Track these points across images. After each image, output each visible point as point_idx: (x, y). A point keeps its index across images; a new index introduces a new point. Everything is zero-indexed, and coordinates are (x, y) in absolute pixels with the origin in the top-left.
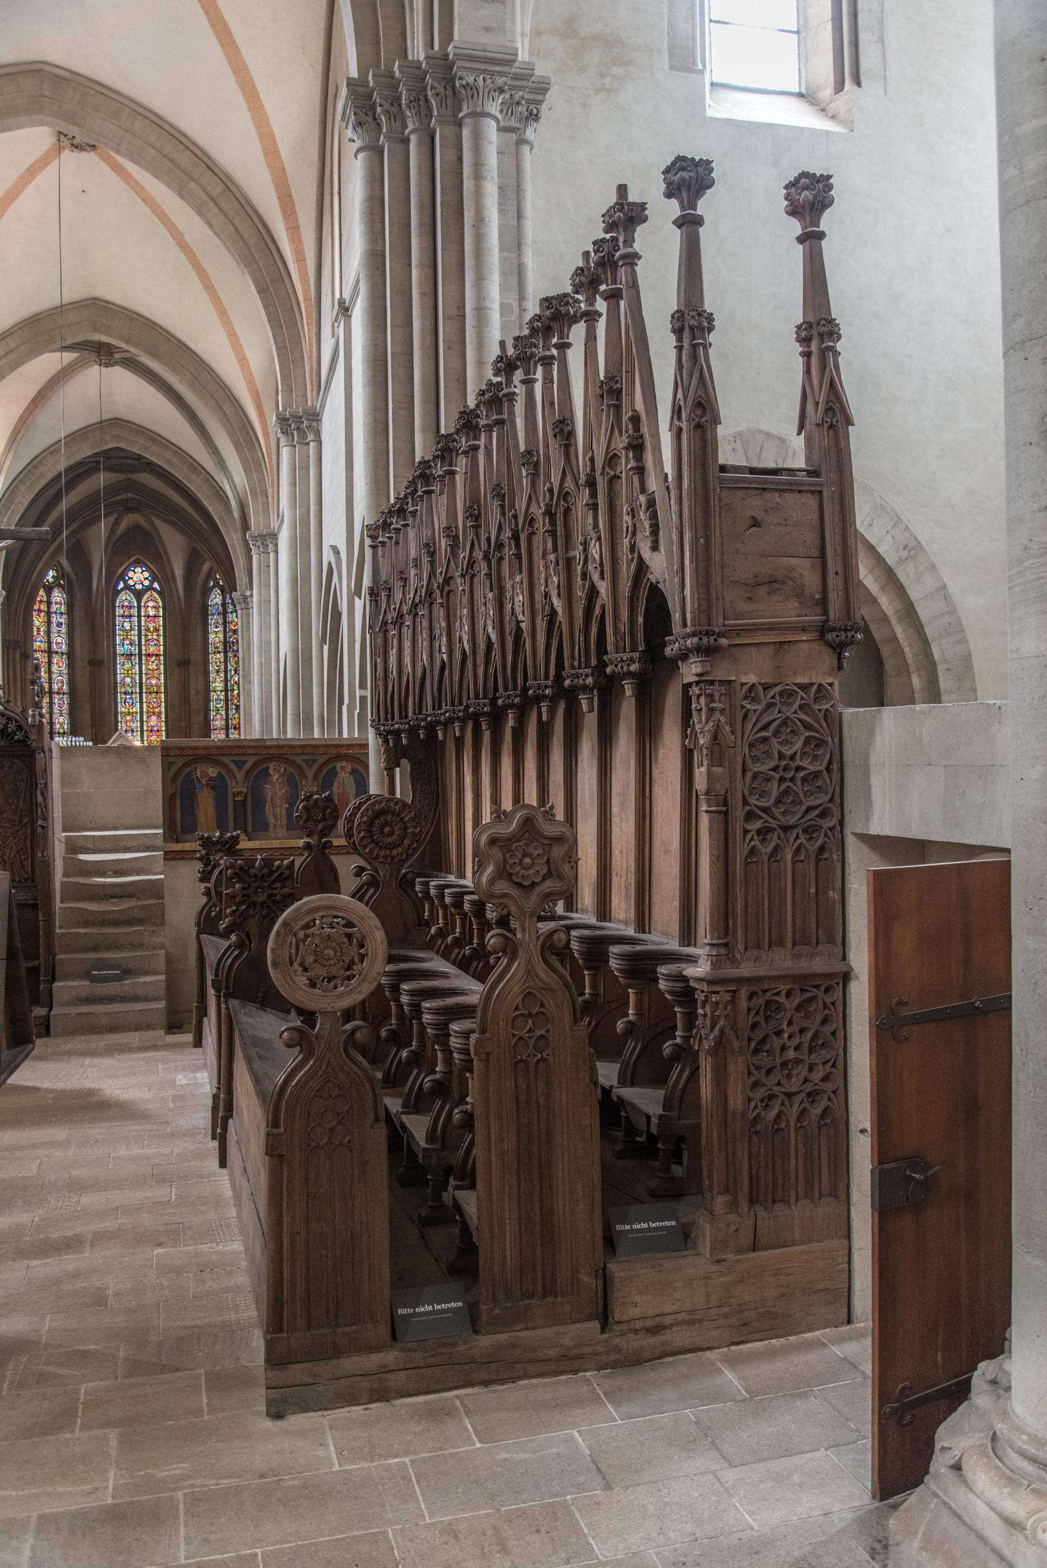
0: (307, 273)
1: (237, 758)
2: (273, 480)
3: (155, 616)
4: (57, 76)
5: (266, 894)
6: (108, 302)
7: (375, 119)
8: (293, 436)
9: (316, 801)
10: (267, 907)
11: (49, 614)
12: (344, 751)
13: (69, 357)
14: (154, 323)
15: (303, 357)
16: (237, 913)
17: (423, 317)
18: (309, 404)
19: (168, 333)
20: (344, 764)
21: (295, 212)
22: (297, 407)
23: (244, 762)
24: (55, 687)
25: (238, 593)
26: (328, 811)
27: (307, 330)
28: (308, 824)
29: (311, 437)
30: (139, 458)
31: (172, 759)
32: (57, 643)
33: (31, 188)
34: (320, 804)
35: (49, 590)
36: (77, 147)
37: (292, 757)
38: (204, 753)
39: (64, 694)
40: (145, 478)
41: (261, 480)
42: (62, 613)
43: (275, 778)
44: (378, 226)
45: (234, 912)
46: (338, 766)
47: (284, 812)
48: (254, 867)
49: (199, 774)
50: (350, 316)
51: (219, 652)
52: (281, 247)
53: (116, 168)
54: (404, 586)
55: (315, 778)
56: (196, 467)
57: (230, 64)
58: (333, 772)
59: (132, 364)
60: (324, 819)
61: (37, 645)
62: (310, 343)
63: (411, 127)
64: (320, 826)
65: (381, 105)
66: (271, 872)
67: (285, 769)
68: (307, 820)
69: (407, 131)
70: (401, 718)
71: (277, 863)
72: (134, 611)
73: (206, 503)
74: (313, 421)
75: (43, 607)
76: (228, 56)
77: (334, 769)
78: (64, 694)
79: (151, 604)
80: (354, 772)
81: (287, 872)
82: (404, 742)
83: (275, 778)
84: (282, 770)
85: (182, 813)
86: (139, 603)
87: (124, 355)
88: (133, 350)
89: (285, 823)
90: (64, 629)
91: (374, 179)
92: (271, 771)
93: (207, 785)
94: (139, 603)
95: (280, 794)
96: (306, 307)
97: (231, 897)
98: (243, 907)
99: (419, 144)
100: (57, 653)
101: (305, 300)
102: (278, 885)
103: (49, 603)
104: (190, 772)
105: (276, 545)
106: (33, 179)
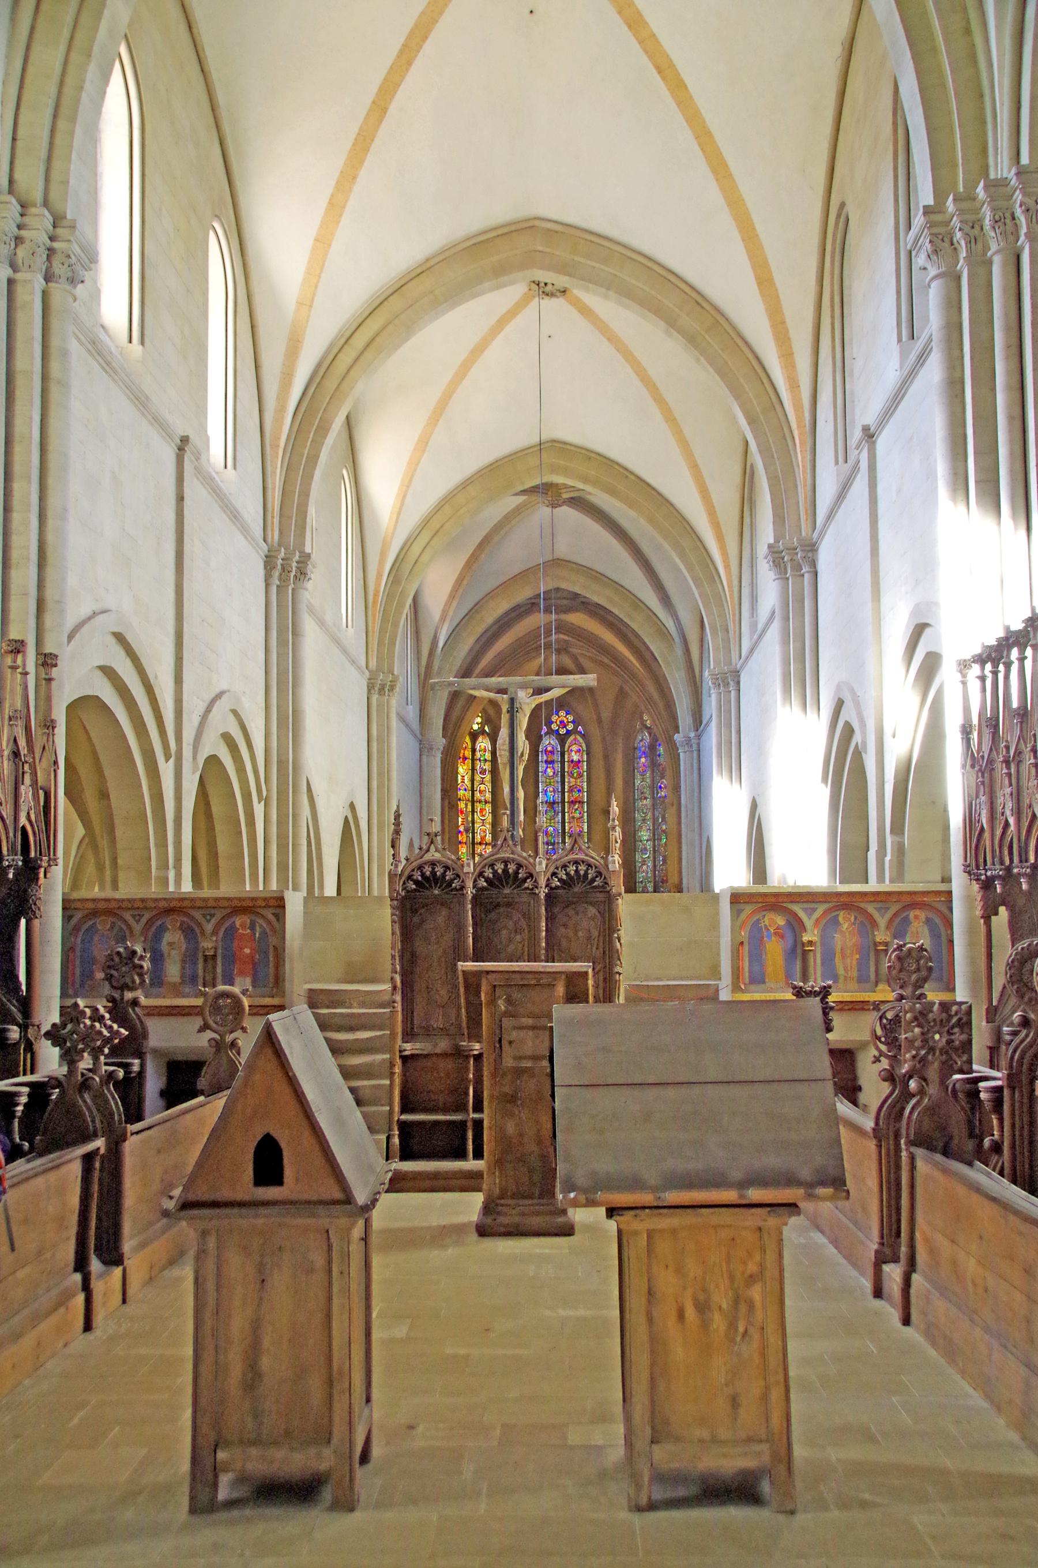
0: (801, 399)
1: (806, 905)
2: (734, 615)
3: (579, 761)
4: (549, 230)
5: (944, 1040)
6: (565, 443)
7: (952, 244)
8: (785, 569)
9: (910, 950)
10: (947, 1053)
11: (473, 760)
12: (918, 899)
13: (521, 499)
14: (612, 461)
15: (796, 486)
16: (918, 1058)
17: (1011, 442)
18: (804, 534)
19: (626, 469)
20: (917, 912)
21: (789, 339)
22: (791, 539)
23: (814, 910)
24: (478, 839)
25: (681, 735)
26: (922, 962)
27: (801, 457)
28: (902, 975)
29: (805, 569)
30: (576, 596)
31: (742, 906)
32: (481, 792)
33: (500, 338)
34: (914, 954)
35: (474, 736)
36: (547, 295)
37: (862, 905)
38: (773, 900)
39: (486, 844)
40: (578, 619)
41: (723, 615)
42: (486, 760)
43: (845, 926)
44: (956, 353)
45: (914, 1057)
46: (912, 914)
47: (855, 963)
48: (932, 1012)
49: (767, 923)
50: (874, 442)
51: (646, 798)
52: (772, 377)
53: (585, 311)
54: (1021, 723)
55: (888, 928)
56: (638, 604)
57: (725, 197)
58: (906, 921)
59: (579, 503)
60: (918, 970)
61: (461, 793)
62: (804, 472)
63: (994, 247)
64: (914, 977)
65: (960, 230)
66: (951, 1017)
67: (856, 918)
68: (900, 971)
69: (989, 254)
70: (1021, 861)
71: (954, 1008)
72: (557, 757)
73: (646, 640)
74: (808, 551)
75: (468, 753)
76: (723, 190)
77: (907, 918)
78: (486, 844)
79: (575, 748)
80: (928, 921)
81: (965, 1019)
82: (1024, 887)
83: (845, 926)
84: (853, 918)
85: (750, 962)
86: (563, 746)
87: (572, 495)
88: (588, 488)
89: (855, 974)
90: (488, 777)
91: (952, 304)
92: (841, 919)
93: (775, 933)
94: (563, 746)
95: (849, 944)
96: (800, 435)
97: (910, 1042)
98: (923, 1052)
99: (1004, 265)
100: (480, 802)
101: (799, 427)
102: (956, 1030)
103: (474, 751)
104: (758, 920)
105: (738, 683)
106: (503, 329)
